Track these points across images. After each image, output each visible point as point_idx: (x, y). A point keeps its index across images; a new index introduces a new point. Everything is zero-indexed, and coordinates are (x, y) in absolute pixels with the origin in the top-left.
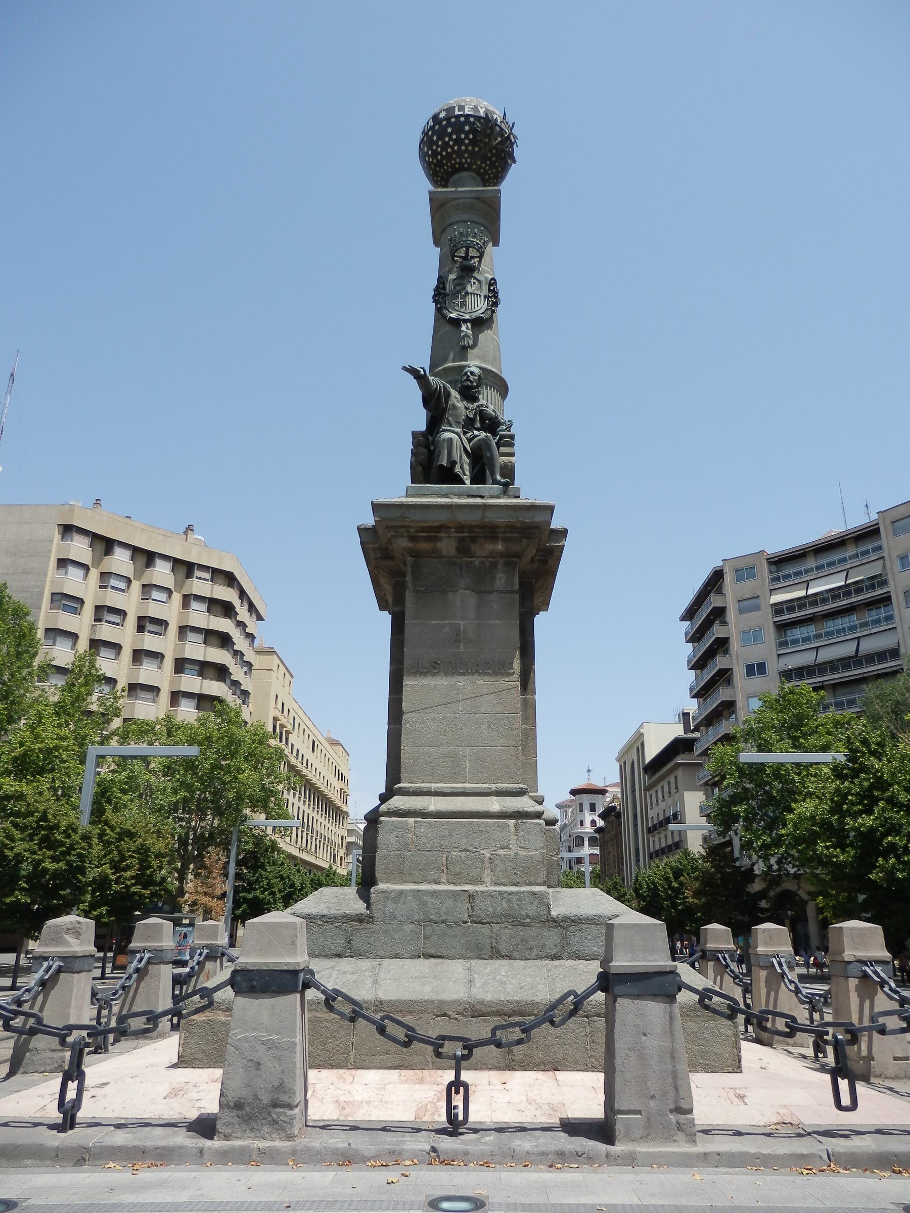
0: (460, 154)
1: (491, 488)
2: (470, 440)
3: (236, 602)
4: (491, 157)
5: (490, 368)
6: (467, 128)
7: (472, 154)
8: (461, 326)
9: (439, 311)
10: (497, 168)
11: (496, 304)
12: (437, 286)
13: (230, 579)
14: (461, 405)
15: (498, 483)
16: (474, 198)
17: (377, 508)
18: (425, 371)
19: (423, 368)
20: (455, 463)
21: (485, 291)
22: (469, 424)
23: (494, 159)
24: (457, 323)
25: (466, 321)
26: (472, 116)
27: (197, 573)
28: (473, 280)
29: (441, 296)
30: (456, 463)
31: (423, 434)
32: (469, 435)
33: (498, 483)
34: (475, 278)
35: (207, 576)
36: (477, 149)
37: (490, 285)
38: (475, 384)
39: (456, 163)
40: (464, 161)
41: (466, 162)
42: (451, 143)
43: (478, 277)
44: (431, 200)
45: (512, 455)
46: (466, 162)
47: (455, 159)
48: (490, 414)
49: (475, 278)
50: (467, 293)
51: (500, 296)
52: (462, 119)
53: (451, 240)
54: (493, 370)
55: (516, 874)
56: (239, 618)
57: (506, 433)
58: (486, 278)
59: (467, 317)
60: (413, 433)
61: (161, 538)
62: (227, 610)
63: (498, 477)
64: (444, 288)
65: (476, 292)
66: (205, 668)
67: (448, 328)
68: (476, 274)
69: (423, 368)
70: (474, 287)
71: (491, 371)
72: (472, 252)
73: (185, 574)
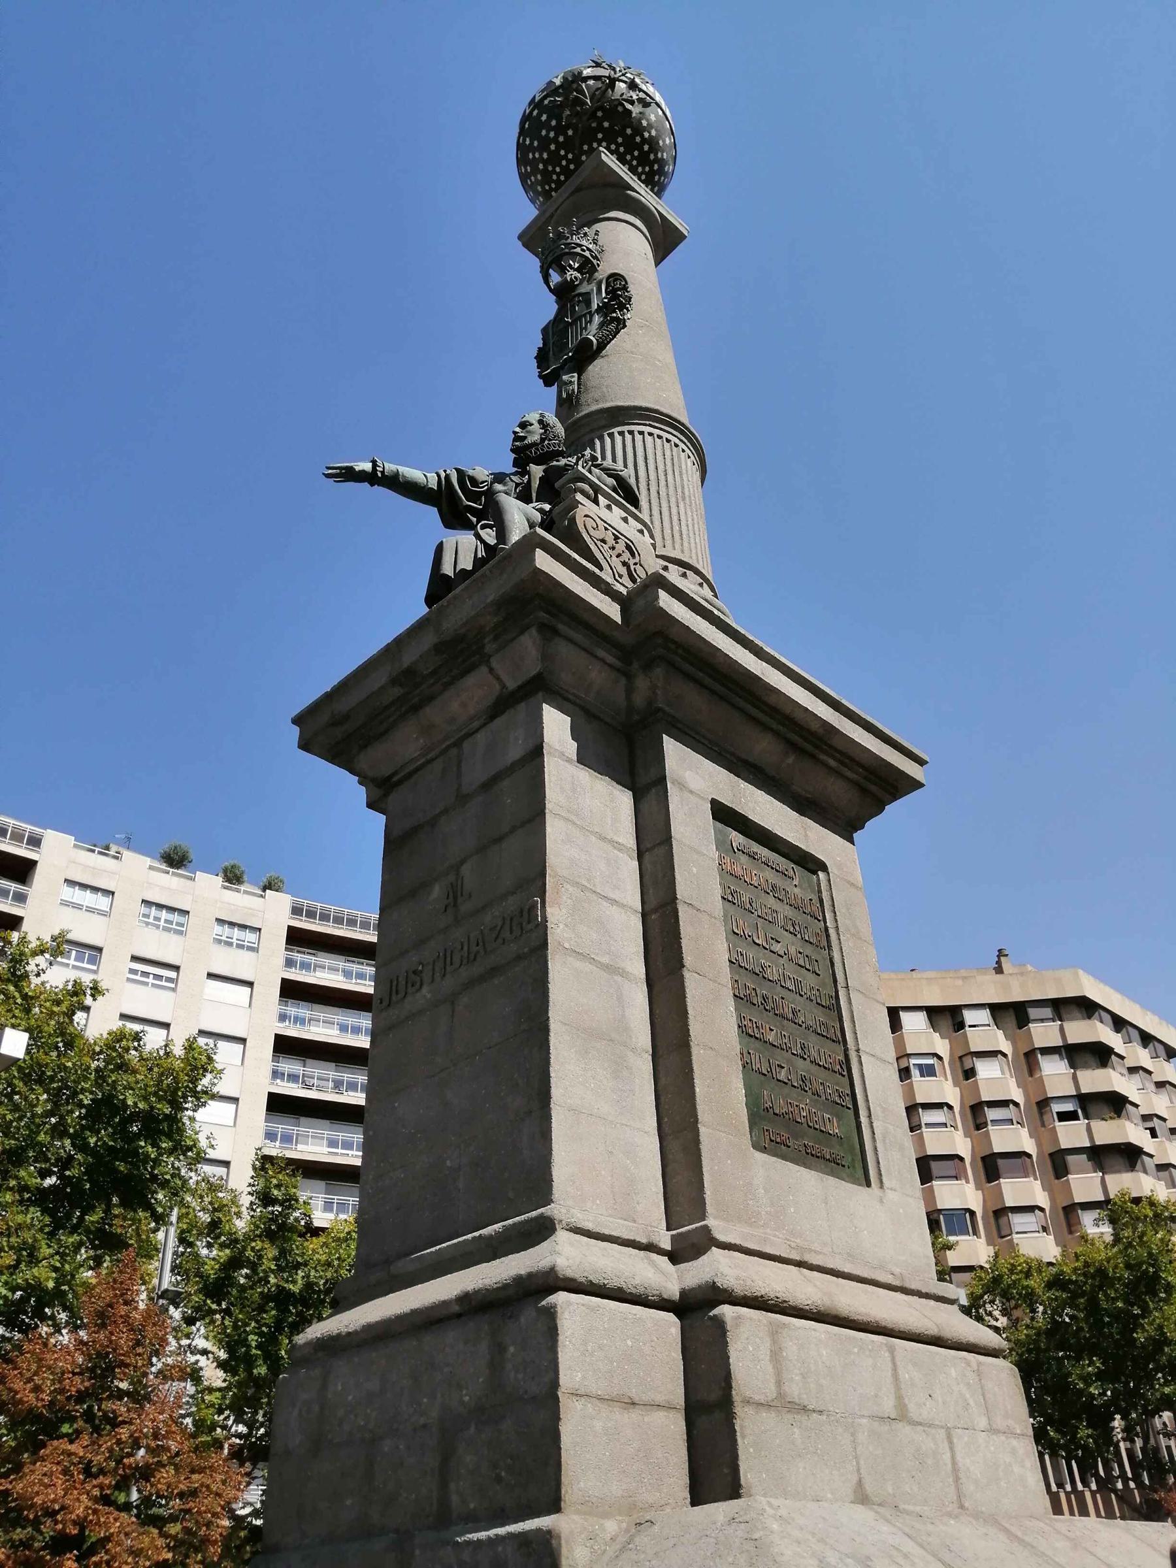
0: (554, 159)
3: (1113, 1040)
4: (600, 125)
6: (544, 117)
7: (568, 145)
10: (622, 133)
13: (1087, 1007)
16: (572, 194)
17: (297, 721)
23: (606, 124)
26: (545, 97)
27: (1033, 1013)
35: (1047, 1012)
36: (570, 133)
38: (536, 438)
39: (558, 175)
40: (564, 163)
41: (569, 162)
42: (537, 155)
44: (526, 245)
46: (569, 162)
47: (554, 171)
52: (535, 113)
55: (499, 1479)
56: (1130, 1063)
61: (960, 982)
62: (1101, 1054)
66: (1106, 1156)
73: (1014, 1022)
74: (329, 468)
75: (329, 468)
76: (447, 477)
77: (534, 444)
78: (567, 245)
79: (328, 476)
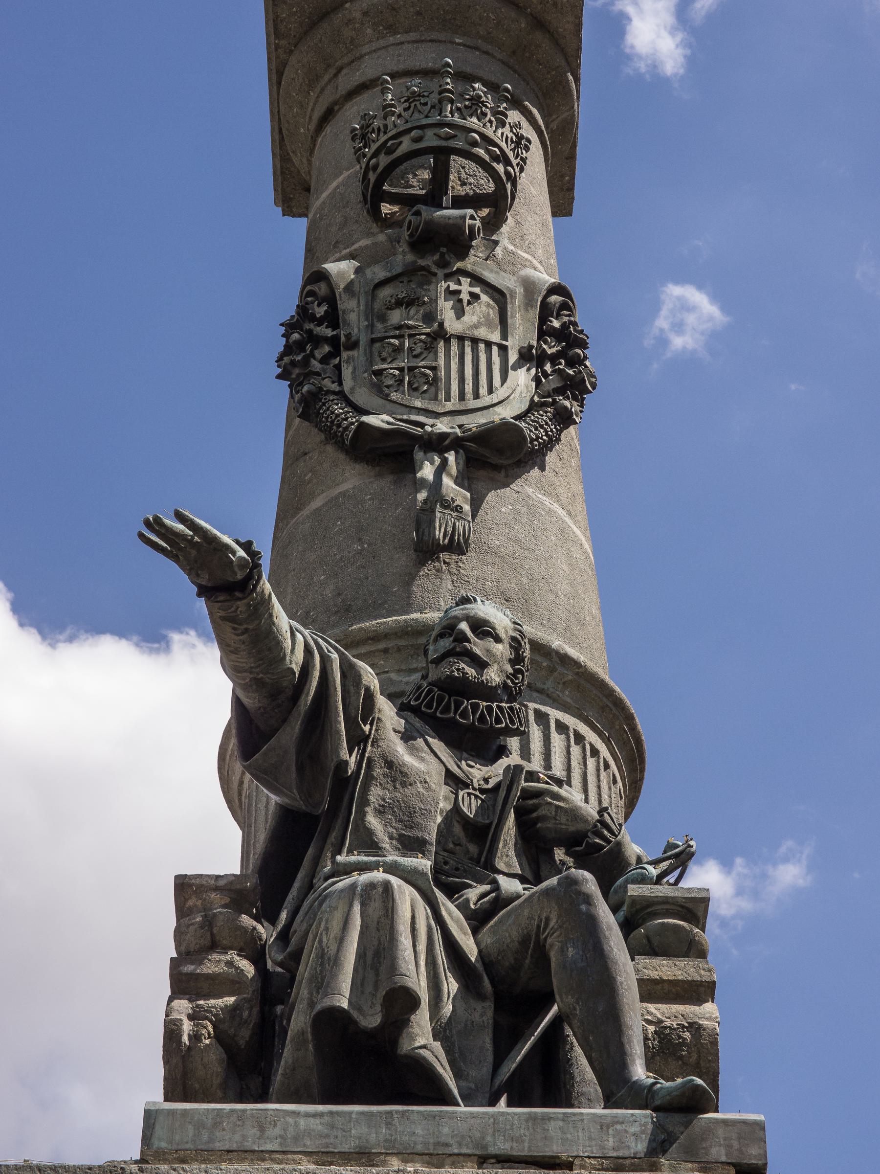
1: (604, 1126)
2: (478, 920)
5: (556, 643)
8: (412, 467)
9: (308, 407)
11: (577, 387)
12: (303, 311)
14: (426, 763)
15: (640, 1097)
18: (254, 555)
19: (247, 546)
20: (402, 1002)
21: (523, 331)
22: (465, 850)
24: (394, 454)
25: (437, 444)
28: (465, 287)
29: (313, 342)
30: (411, 1001)
31: (231, 890)
32: (474, 893)
33: (640, 1097)
34: (477, 279)
37: (546, 312)
38: (493, 676)
43: (490, 276)
45: (699, 992)
48: (574, 814)
49: (477, 279)
50: (441, 334)
51: (593, 361)
53: (363, 136)
54: (573, 652)
57: (662, 891)
58: (529, 286)
59: (442, 426)
60: (185, 886)
63: (639, 1072)
64: (333, 318)
65: (482, 333)
67: (351, 479)
68: (474, 261)
69: (247, 546)
70: (472, 316)
71: (565, 659)
72: (465, 176)
74: (180, 517)
75: (180, 517)
76: (325, 660)
77: (488, 692)
78: (488, 141)
79: (156, 525)
